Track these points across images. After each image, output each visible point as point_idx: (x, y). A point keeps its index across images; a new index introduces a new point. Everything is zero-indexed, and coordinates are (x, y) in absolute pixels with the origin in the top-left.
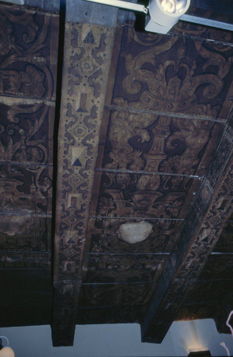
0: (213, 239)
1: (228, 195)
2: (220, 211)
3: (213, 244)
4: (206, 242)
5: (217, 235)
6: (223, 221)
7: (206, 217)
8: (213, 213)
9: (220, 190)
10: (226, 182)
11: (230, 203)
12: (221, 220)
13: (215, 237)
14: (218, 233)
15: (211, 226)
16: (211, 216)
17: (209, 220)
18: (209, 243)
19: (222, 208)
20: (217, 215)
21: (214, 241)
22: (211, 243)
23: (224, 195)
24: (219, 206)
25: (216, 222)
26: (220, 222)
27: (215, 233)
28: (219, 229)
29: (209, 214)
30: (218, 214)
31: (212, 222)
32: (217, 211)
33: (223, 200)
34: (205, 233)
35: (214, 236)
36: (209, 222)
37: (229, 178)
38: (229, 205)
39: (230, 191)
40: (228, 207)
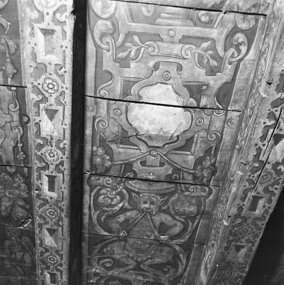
0: (263, 138)
1: (250, 218)
2: (258, 193)
3: (263, 126)
4: (275, 132)
5: (257, 147)
6: (250, 176)
7: (280, 185)
8: (269, 190)
9: (263, 224)
10: (257, 234)
11: (245, 206)
12: (254, 179)
13: (260, 144)
14: (255, 154)
15: (271, 167)
16: (272, 185)
17: (274, 178)
18: (271, 131)
19: (256, 199)
20: (263, 187)
21: (261, 135)
22: (267, 128)
23: (257, 218)
24: (261, 203)
25: (263, 174)
26: (256, 175)
27: (262, 153)
28: (254, 161)
29: (276, 189)
30: (260, 188)
31: (269, 176)
32: (262, 193)
33: (256, 211)
34: (280, 155)
35: (262, 147)
36: (274, 175)
37: (252, 239)
38: (245, 203)
39: (248, 222)
40: (247, 199)
